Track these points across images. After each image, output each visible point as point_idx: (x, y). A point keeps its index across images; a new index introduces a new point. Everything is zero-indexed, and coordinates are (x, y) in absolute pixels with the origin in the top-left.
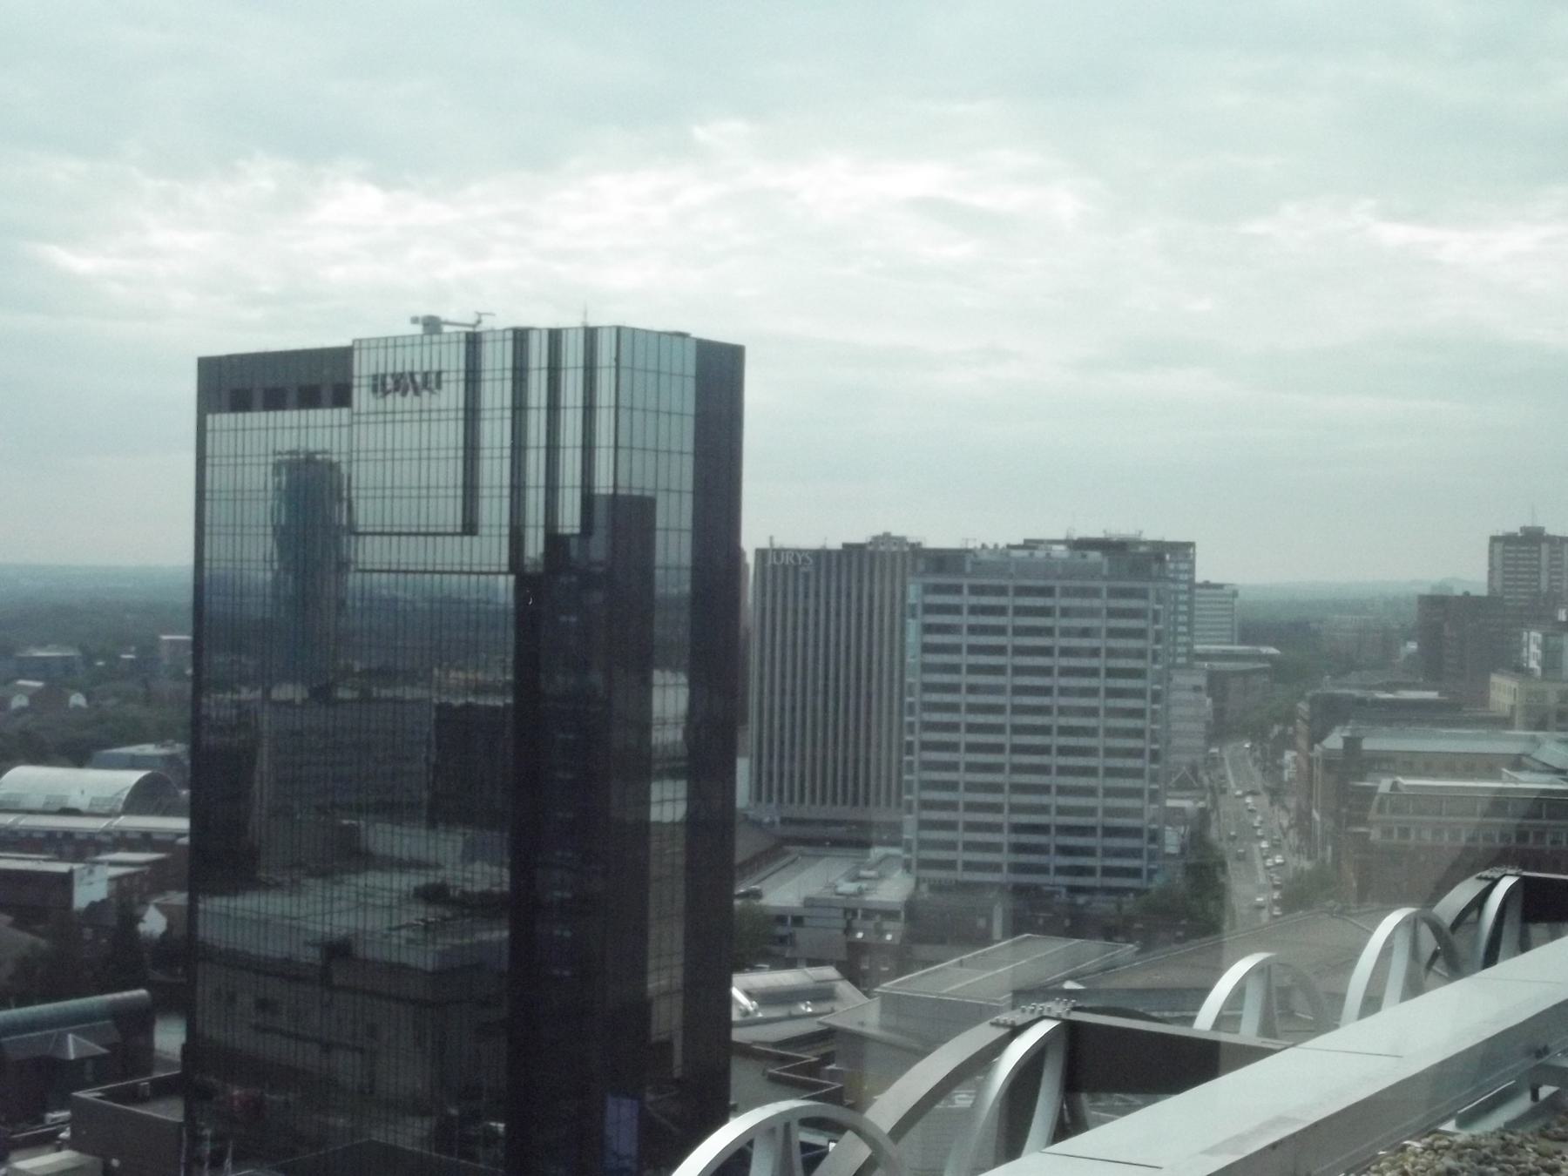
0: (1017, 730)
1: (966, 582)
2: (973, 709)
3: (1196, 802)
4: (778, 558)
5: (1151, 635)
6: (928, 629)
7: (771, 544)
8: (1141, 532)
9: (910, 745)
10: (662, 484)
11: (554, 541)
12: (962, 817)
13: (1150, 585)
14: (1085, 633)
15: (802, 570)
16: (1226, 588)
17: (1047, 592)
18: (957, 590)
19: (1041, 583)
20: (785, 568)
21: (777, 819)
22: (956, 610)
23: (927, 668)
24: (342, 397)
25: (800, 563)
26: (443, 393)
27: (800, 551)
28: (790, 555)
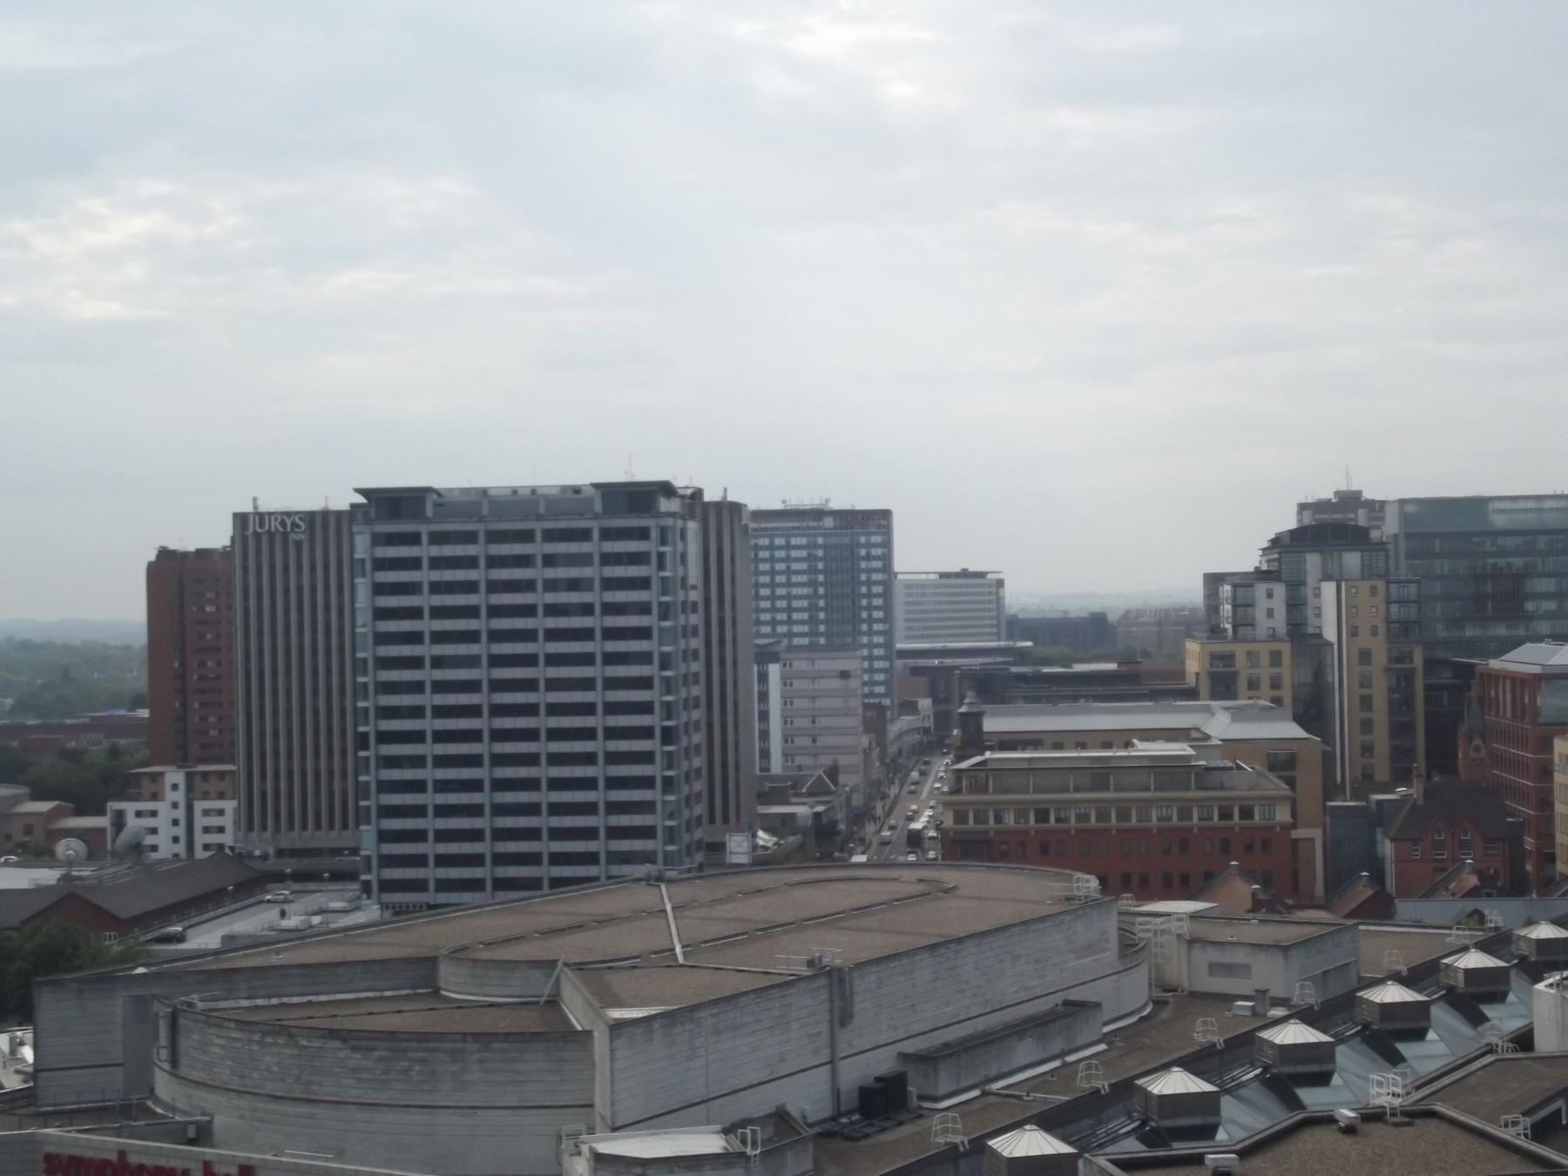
0: (612, 733)
1: (424, 529)
2: (440, 687)
3: (812, 807)
4: (262, 525)
5: (655, 584)
6: (379, 589)
7: (256, 507)
8: (827, 501)
9: (365, 736)
14: (574, 585)
15: (293, 537)
17: (526, 536)
18: (414, 539)
19: (518, 526)
20: (271, 535)
21: (271, 851)
22: (414, 564)
23: (382, 639)
25: (289, 529)
27: (288, 514)
28: (276, 519)
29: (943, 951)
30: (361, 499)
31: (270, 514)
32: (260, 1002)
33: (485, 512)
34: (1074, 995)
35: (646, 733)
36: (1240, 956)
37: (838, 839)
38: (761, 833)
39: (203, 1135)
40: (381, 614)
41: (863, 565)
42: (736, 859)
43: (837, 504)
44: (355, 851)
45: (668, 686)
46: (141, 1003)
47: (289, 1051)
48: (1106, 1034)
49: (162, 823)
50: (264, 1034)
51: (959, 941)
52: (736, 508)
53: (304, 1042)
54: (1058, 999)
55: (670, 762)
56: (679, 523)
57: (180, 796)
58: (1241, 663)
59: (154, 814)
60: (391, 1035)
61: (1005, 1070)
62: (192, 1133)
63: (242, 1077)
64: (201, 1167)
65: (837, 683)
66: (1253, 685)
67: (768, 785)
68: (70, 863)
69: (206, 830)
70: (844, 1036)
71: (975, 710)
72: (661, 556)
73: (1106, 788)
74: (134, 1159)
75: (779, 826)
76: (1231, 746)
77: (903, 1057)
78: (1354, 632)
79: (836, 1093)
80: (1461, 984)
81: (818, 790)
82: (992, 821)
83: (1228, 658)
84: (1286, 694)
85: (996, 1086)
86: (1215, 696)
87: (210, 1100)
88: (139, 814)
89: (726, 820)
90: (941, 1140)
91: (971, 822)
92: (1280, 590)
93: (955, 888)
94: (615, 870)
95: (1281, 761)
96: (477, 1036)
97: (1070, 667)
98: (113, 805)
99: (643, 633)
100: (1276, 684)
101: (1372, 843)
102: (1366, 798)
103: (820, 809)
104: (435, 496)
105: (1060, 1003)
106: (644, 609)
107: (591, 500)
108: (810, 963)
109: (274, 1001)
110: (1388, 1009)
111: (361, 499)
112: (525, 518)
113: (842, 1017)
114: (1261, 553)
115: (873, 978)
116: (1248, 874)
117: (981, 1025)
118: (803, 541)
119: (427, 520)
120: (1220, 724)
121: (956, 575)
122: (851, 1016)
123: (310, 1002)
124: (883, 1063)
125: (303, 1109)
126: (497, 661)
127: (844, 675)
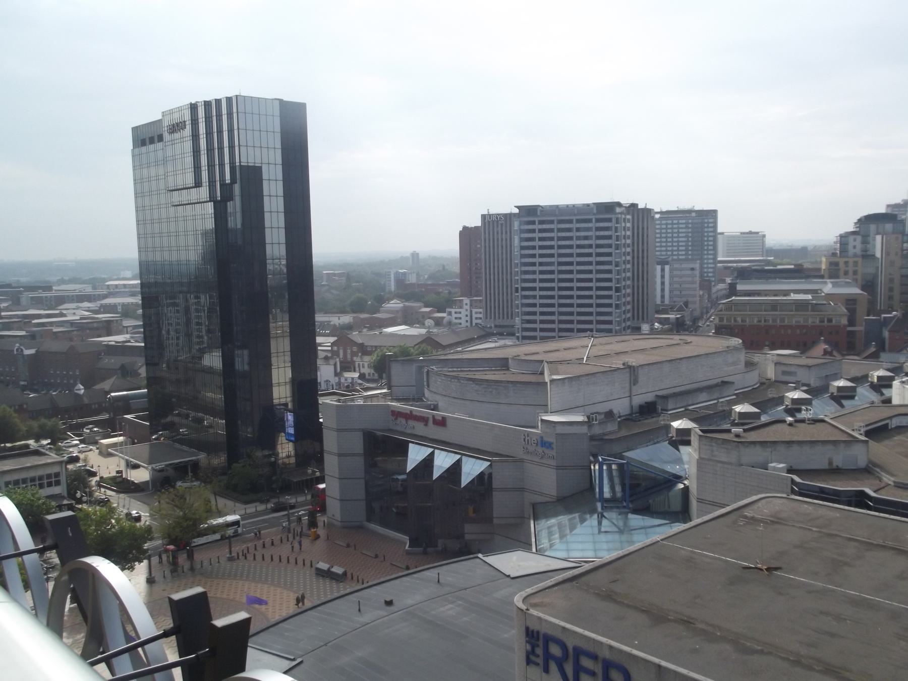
1: (537, 219)
4: (490, 218)
7: (488, 212)
8: (694, 206)
9: (517, 289)
10: (265, 160)
11: (223, 185)
12: (538, 318)
13: (613, 216)
14: (586, 238)
15: (500, 222)
16: (760, 233)
19: (567, 218)
21: (493, 326)
23: (523, 256)
24: (160, 138)
26: (186, 130)
27: (499, 214)
29: (674, 362)
30: (516, 211)
31: (493, 215)
32: (455, 369)
33: (557, 213)
34: (726, 379)
35: (610, 289)
36: (793, 369)
37: (686, 327)
38: (656, 324)
39: (435, 408)
40: (522, 248)
41: (706, 230)
42: (644, 332)
43: (697, 208)
44: (513, 326)
45: (618, 273)
46: (420, 369)
47: (458, 384)
48: (736, 394)
49: (462, 315)
50: (452, 378)
51: (681, 359)
52: (647, 212)
53: (462, 382)
54: (719, 380)
55: (619, 298)
56: (623, 216)
57: (468, 307)
58: (842, 265)
59: (460, 313)
60: (487, 381)
61: (695, 402)
62: (432, 407)
63: (446, 391)
64: (432, 416)
65: (690, 272)
66: (846, 273)
67: (661, 308)
68: (429, 327)
69: (476, 318)
70: (634, 388)
71: (734, 282)
72: (616, 228)
73: (776, 310)
74: (414, 413)
75: (661, 321)
76: (830, 296)
77: (657, 396)
78: (888, 254)
79: (632, 407)
80: (875, 380)
81: (680, 310)
82: (733, 321)
83: (837, 264)
84: (859, 277)
85: (690, 408)
86: (830, 277)
87: (438, 397)
88: (456, 313)
89: (643, 319)
90: (662, 423)
91: (725, 321)
92: (859, 238)
93: (691, 342)
94: (561, 334)
95: (850, 302)
96: (512, 382)
97: (776, 267)
98: (448, 310)
99: (610, 254)
100: (855, 273)
101: (881, 332)
102: (880, 316)
103: (678, 316)
104: (541, 208)
105: (720, 382)
106: (610, 246)
107: (592, 208)
108: (624, 364)
109: (459, 369)
110: (840, 389)
111: (516, 211)
112: (570, 215)
113: (634, 381)
114: (854, 224)
115: (646, 370)
116: (826, 342)
117: (688, 387)
118: (684, 221)
119: (538, 216)
120: (828, 288)
121: (747, 233)
122: (638, 382)
123: (470, 370)
124: (650, 398)
125: (462, 402)
126: (560, 264)
127: (692, 269)
